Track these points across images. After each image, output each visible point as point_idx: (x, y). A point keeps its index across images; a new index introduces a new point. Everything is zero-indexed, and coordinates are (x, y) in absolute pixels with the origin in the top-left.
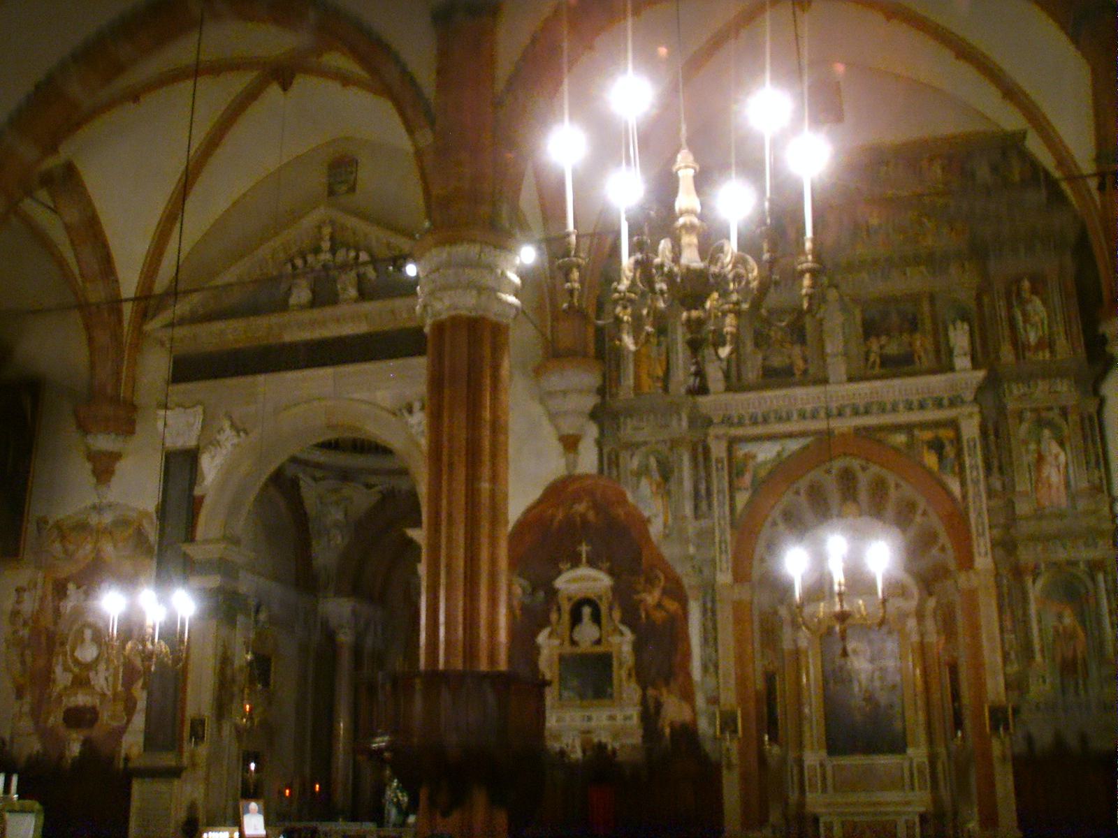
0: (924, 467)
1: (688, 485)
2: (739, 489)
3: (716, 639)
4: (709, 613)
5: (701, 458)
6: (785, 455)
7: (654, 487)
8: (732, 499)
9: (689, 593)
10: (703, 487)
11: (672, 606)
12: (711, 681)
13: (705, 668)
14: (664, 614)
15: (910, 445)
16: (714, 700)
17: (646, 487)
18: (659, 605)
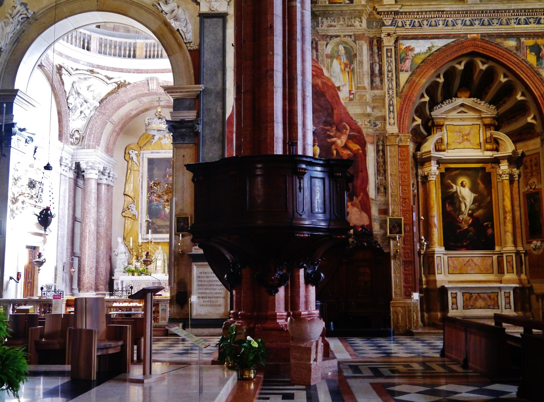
0: (527, 62)
1: (366, 67)
2: (402, 71)
3: (385, 171)
4: (381, 153)
5: (375, 49)
6: (434, 49)
7: (343, 67)
8: (397, 78)
9: (367, 139)
10: (377, 69)
11: (355, 147)
12: (381, 199)
13: (378, 189)
14: (349, 152)
15: (518, 48)
16: (384, 212)
17: (336, 65)
18: (346, 147)
